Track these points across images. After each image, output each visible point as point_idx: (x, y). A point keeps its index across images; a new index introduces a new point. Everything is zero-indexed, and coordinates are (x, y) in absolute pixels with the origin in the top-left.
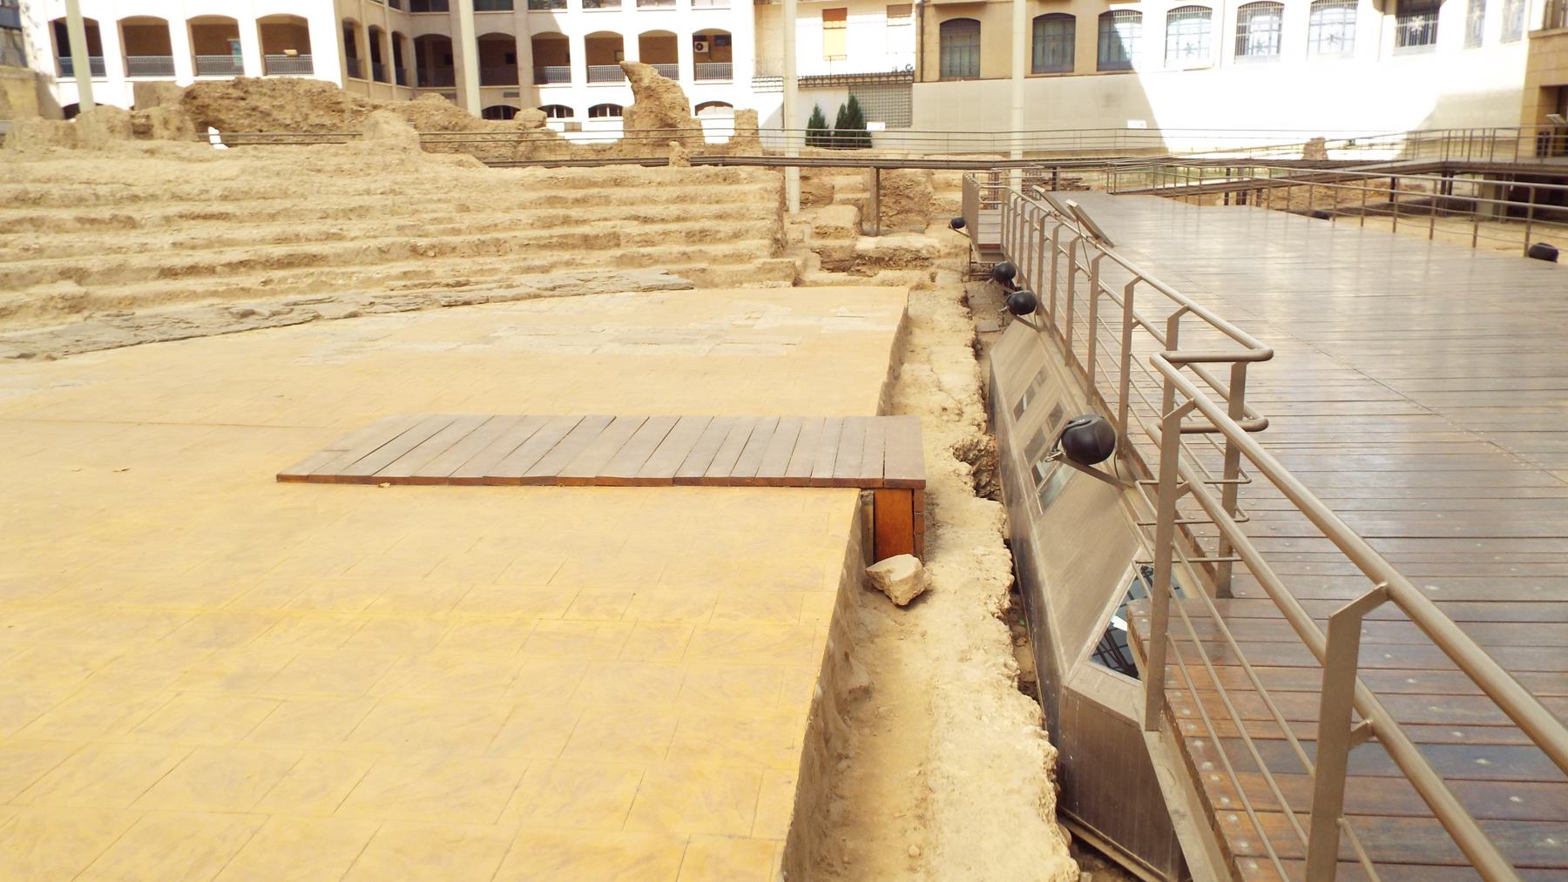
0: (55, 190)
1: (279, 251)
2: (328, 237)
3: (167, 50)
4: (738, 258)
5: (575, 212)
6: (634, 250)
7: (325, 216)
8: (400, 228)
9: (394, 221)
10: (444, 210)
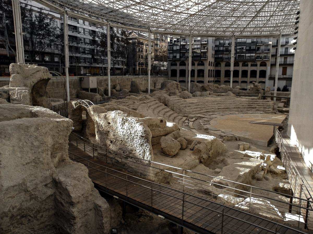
1: (226, 107)
4: (269, 111)
5: (252, 104)
10: (239, 104)
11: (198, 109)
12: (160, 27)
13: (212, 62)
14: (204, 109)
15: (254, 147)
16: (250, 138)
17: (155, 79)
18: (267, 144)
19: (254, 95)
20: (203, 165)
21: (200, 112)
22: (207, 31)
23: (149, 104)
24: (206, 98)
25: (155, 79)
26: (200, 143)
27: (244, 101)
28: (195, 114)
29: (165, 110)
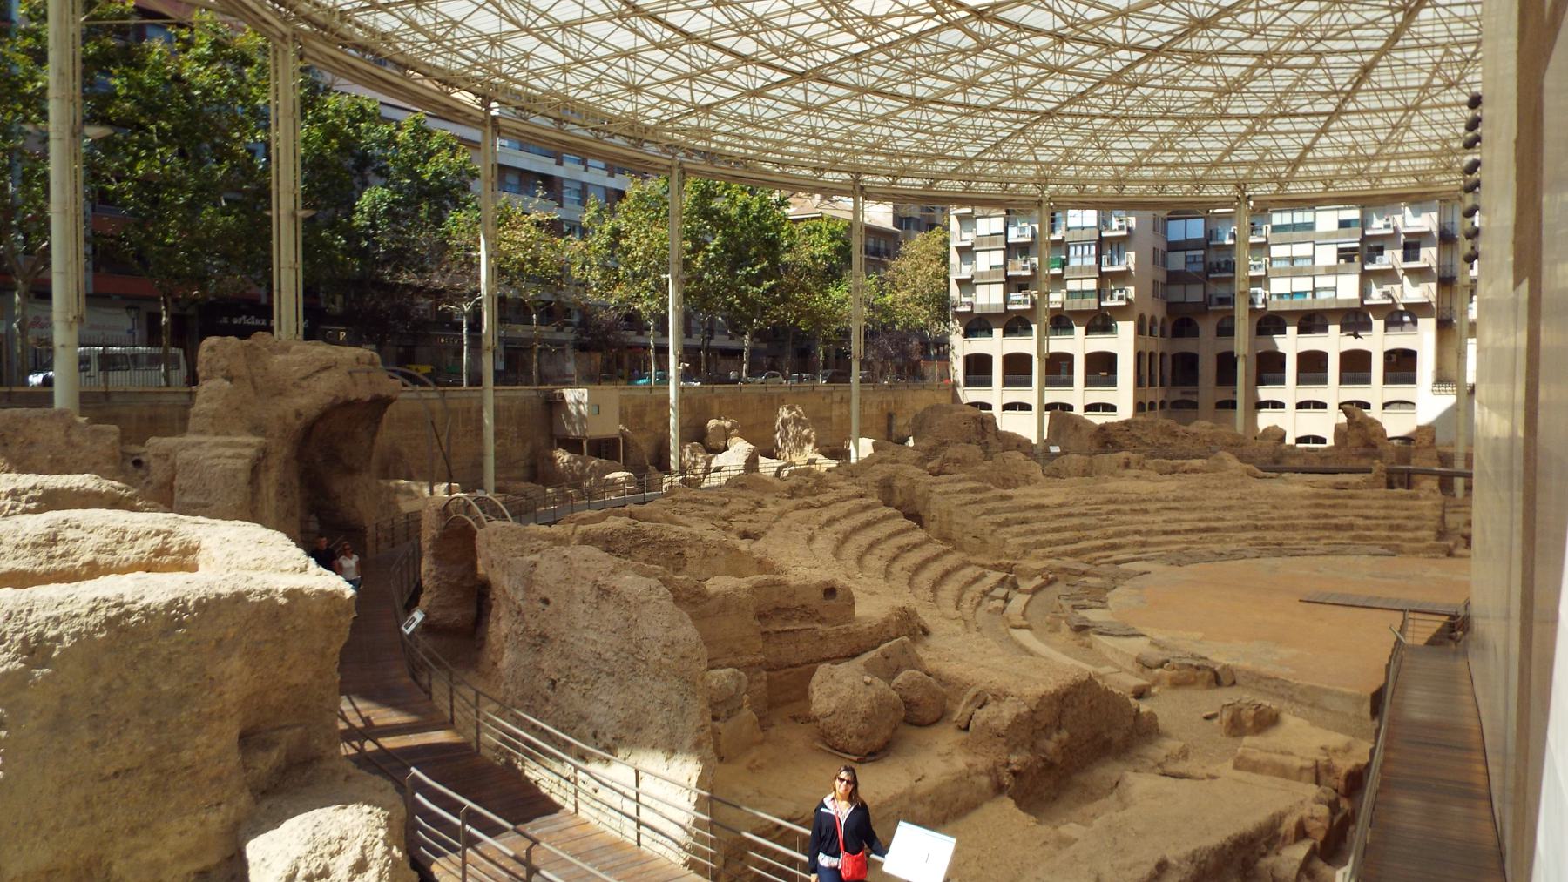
0: (1120, 497)
1: (1202, 525)
2: (1218, 519)
3: (1030, 373)
4: (1417, 540)
5: (1330, 512)
6: (1361, 532)
7: (1215, 509)
8: (1249, 517)
9: (1245, 513)
10: (1266, 508)
11: (1067, 535)
12: (904, 172)
13: (1153, 319)
14: (1094, 534)
15: (1298, 721)
16: (1284, 672)
17: (890, 398)
18: (1367, 707)
19: (1350, 465)
20: (1009, 804)
21: (1074, 547)
22: (1120, 182)
23: (826, 514)
24: (1106, 481)
25: (890, 398)
26: (1006, 695)
27: (1294, 496)
28: (1049, 557)
29: (903, 540)
